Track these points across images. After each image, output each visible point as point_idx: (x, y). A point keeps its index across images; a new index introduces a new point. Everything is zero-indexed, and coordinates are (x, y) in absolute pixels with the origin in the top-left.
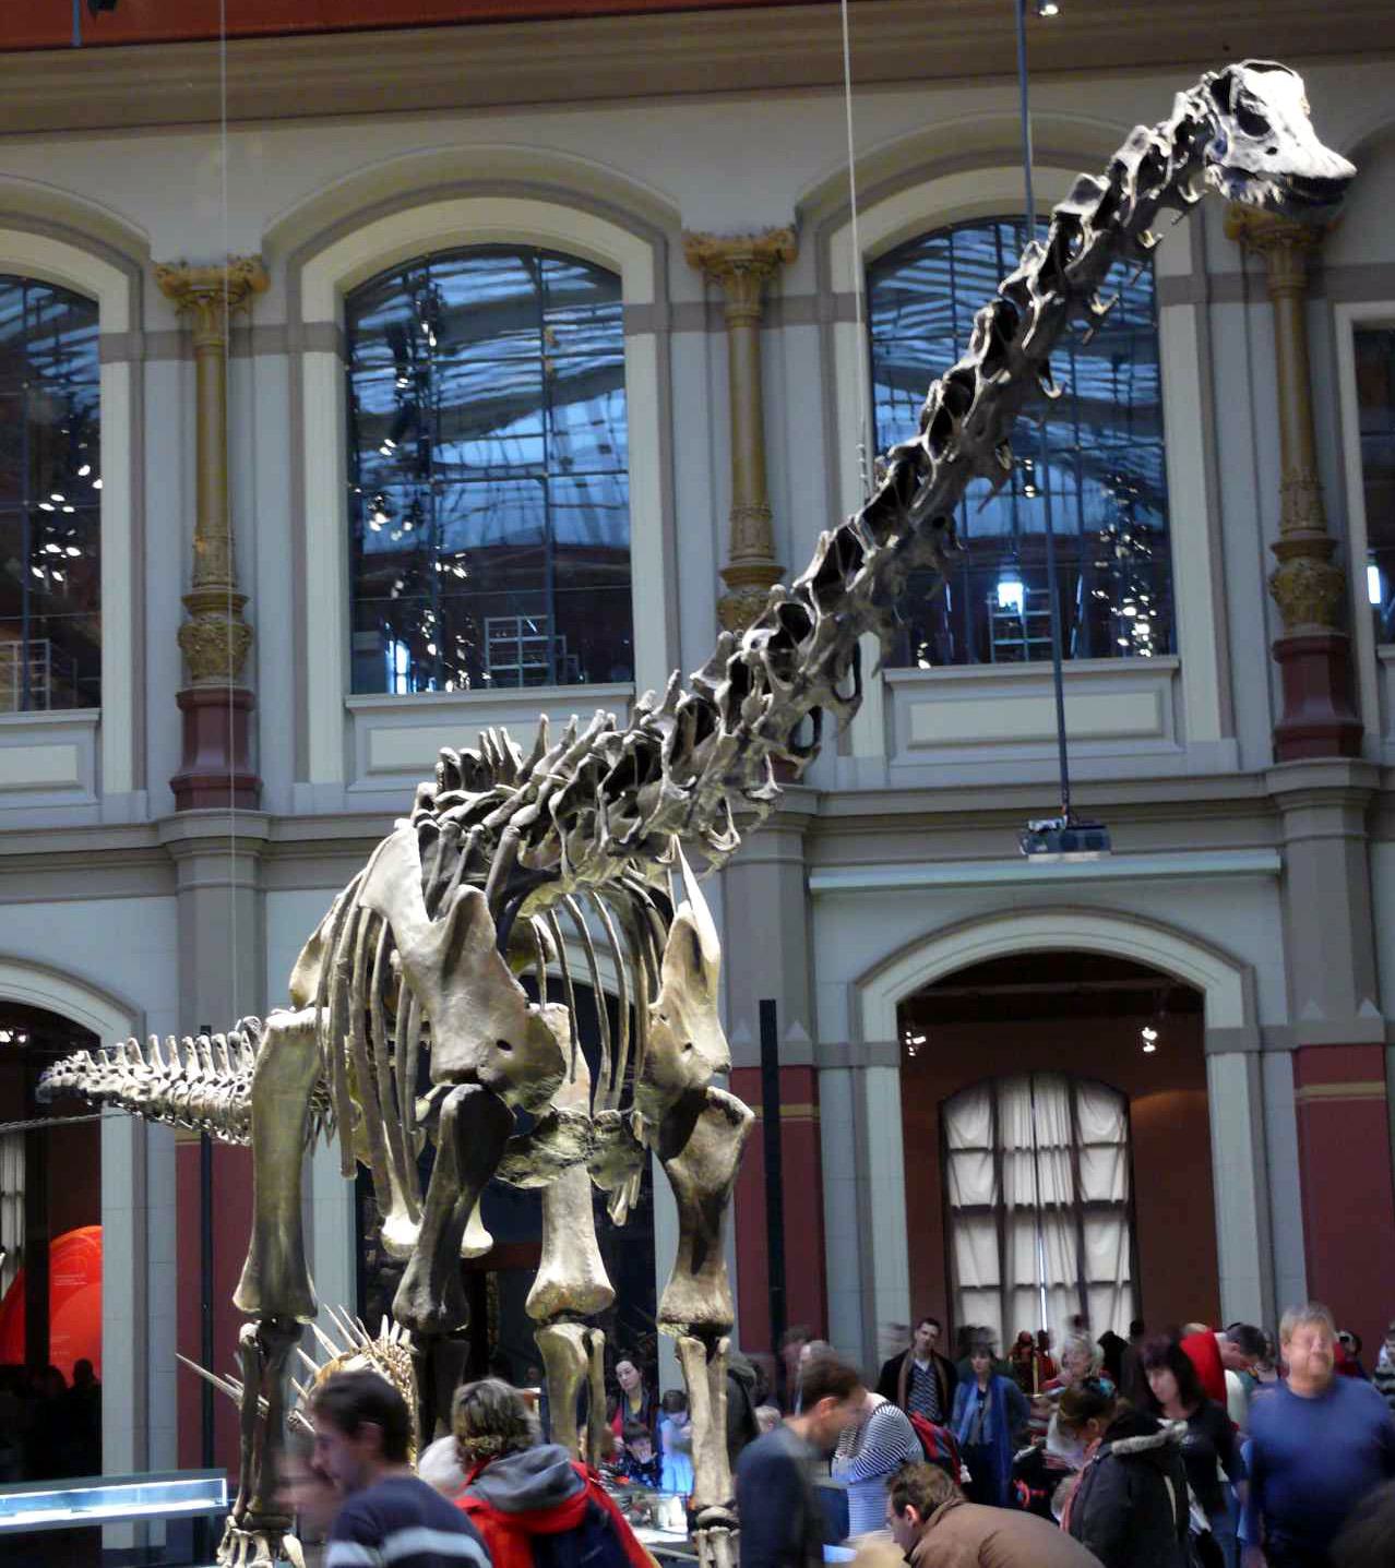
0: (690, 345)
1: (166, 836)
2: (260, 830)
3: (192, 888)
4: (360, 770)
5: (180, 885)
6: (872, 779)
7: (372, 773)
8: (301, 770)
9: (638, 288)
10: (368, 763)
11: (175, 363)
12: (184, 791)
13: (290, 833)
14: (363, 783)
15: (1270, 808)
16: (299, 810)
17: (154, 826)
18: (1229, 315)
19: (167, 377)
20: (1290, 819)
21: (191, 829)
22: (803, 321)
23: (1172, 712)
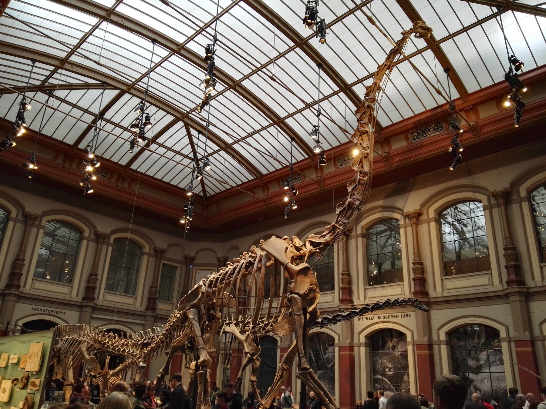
0: (91, 243)
1: (5, 292)
2: (20, 294)
3: (9, 300)
4: (32, 288)
5: (5, 299)
6: (100, 304)
7: (34, 289)
8: (25, 286)
9: (86, 234)
10: (34, 286)
11: (21, 224)
12: (9, 286)
13: (23, 295)
14: (32, 290)
15: (145, 316)
16: (23, 292)
17: (3, 290)
18: (151, 258)
19: (20, 227)
20: (147, 318)
21: (12, 292)
22: (105, 245)
23: (135, 303)
